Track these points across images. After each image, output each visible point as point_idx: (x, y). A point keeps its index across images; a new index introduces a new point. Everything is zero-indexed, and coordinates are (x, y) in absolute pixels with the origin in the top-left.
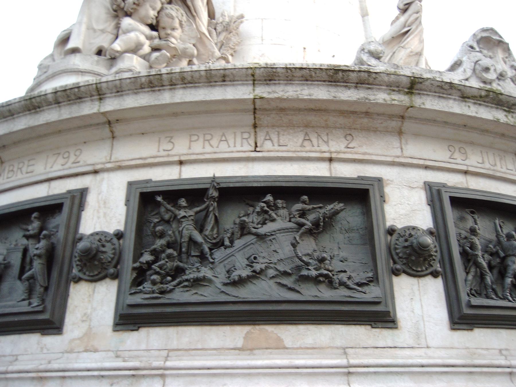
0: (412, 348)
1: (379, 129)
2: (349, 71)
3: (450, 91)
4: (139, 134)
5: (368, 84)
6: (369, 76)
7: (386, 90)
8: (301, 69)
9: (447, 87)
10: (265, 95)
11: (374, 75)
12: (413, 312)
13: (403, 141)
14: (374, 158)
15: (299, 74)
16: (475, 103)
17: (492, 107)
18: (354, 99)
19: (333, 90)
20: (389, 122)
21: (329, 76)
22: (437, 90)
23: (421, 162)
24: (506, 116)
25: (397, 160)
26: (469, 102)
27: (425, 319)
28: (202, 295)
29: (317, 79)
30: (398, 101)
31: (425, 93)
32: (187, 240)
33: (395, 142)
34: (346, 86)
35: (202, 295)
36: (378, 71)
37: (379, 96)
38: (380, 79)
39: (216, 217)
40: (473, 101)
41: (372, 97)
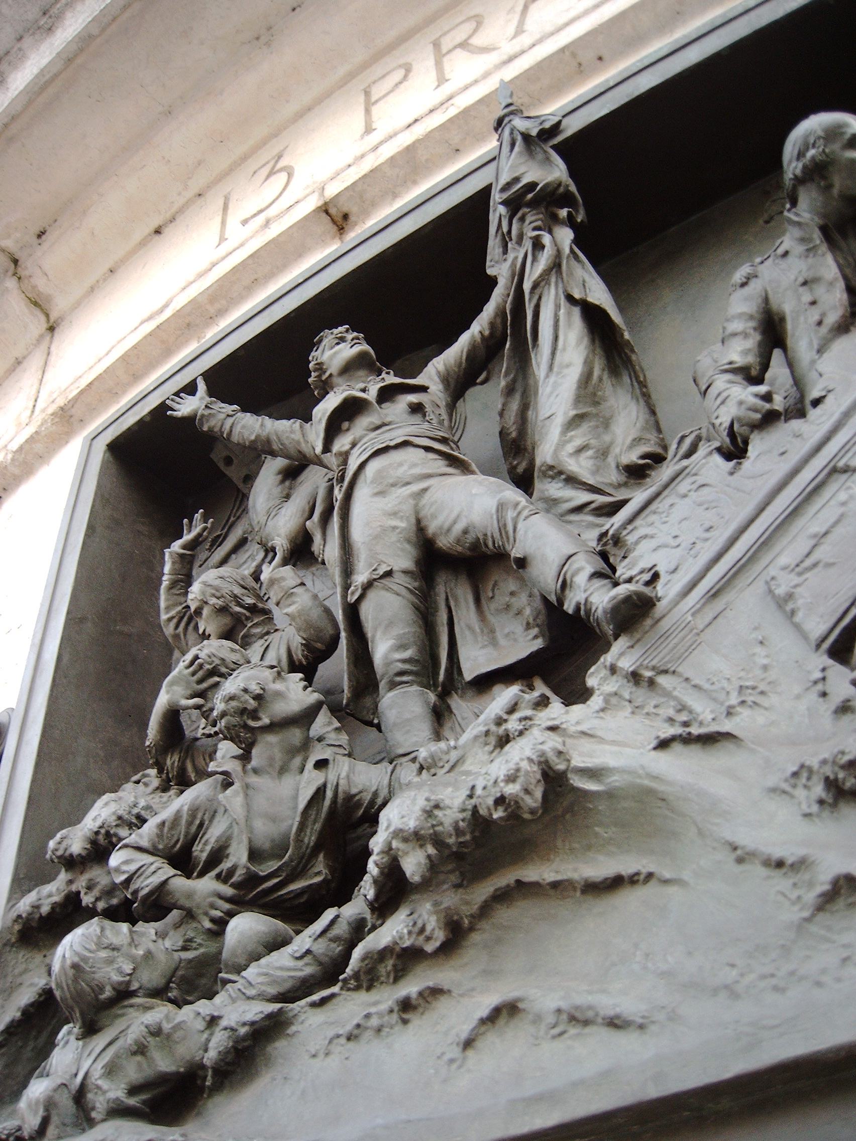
4: (143, 243)
28: (578, 1019)
32: (402, 559)
35: (578, 1019)
39: (593, 316)
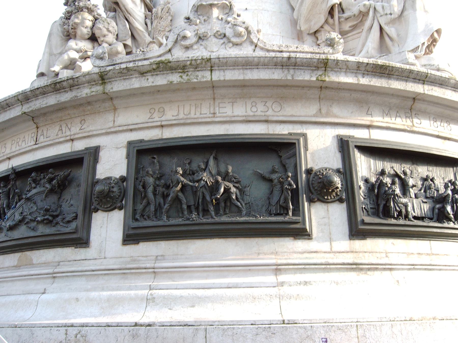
0: (95, 259)
1: (101, 111)
2: (61, 81)
3: (129, 73)
5: (77, 86)
6: (73, 81)
7: (88, 86)
8: (38, 89)
9: (125, 71)
10: (26, 111)
11: (76, 80)
12: (100, 235)
13: (116, 115)
14: (95, 133)
15: (38, 92)
16: (152, 75)
17: (167, 74)
18: (69, 99)
19: (58, 96)
20: (104, 104)
21: (53, 88)
22: (120, 75)
23: (125, 128)
24: (181, 77)
25: (109, 130)
26: (147, 76)
27: (107, 240)
29: (48, 92)
30: (95, 92)
31: (113, 80)
33: (110, 117)
34: (65, 91)
36: (78, 76)
37: (84, 92)
38: (80, 81)
40: (150, 74)
41: (79, 95)
